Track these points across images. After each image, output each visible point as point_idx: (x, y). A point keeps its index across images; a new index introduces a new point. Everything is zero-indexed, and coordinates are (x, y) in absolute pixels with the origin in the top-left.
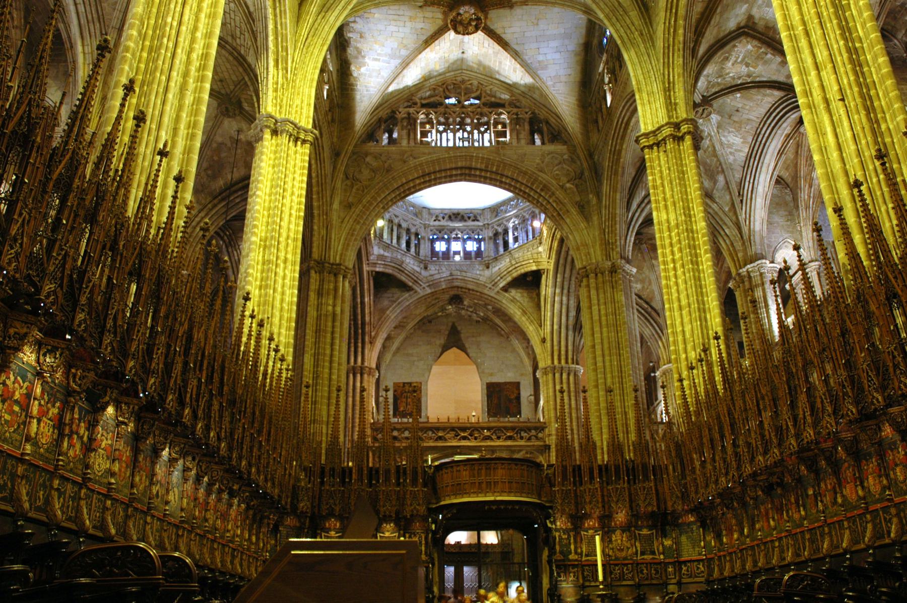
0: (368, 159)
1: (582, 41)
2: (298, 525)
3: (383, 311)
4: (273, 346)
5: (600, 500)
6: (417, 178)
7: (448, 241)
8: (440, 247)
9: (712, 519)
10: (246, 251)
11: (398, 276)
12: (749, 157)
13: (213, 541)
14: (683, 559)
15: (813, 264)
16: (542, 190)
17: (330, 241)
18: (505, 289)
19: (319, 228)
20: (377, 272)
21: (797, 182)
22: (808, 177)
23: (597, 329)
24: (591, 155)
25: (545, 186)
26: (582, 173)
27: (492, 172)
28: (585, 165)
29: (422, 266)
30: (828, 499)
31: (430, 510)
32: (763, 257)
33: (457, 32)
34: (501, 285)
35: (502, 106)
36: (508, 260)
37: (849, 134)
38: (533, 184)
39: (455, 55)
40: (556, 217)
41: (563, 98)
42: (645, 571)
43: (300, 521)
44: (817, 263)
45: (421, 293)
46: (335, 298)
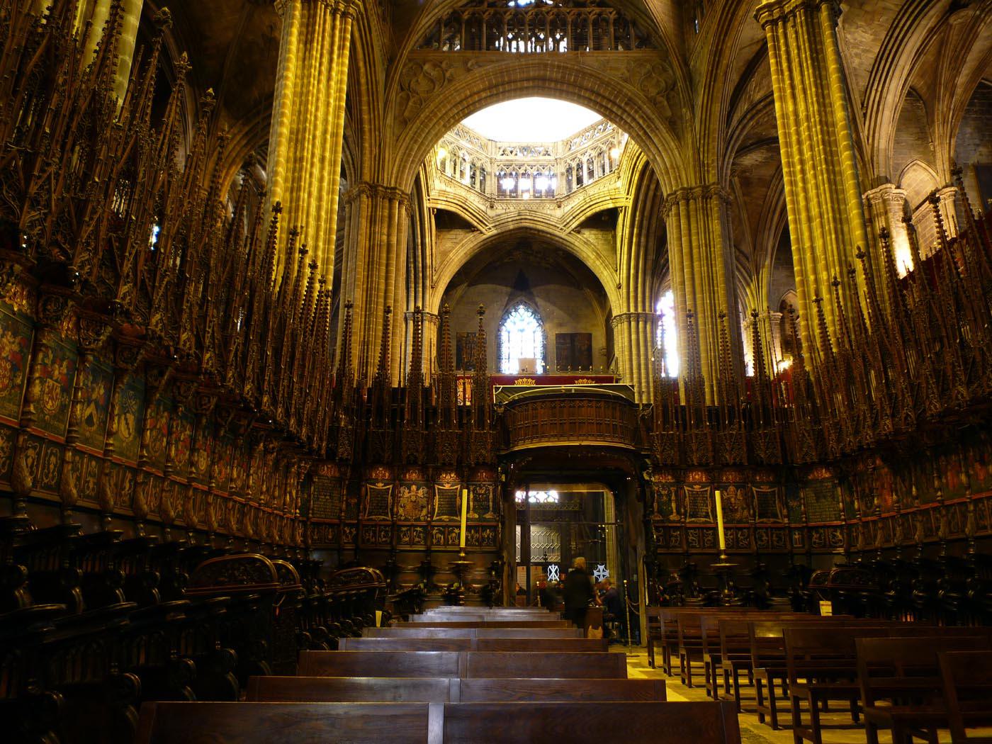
0: (426, 67)
2: (337, 475)
4: (308, 261)
5: (711, 449)
6: (484, 90)
8: (508, 184)
9: (855, 475)
10: (274, 145)
12: (879, 59)
13: (208, 493)
14: (812, 524)
15: (949, 189)
16: (626, 104)
17: (384, 161)
19: (371, 147)
20: (438, 210)
21: (934, 91)
22: (950, 85)
25: (630, 99)
26: (675, 84)
27: (569, 84)
28: (679, 73)
29: (488, 204)
32: (888, 181)
34: (573, 226)
36: (582, 198)
38: (616, 97)
40: (642, 137)
42: (765, 538)
43: (339, 471)
44: (953, 189)
46: (390, 226)
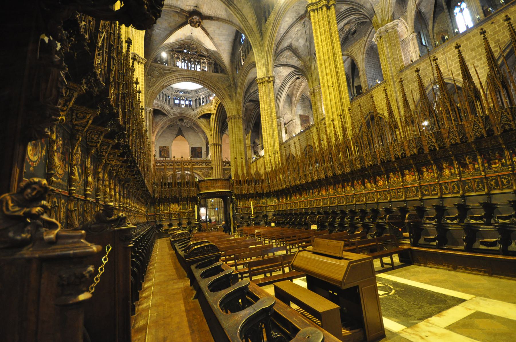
1: (233, 38)
3: (157, 123)
7: (180, 100)
8: (177, 102)
11: (162, 111)
12: (281, 87)
18: (199, 118)
23: (234, 136)
24: (234, 80)
26: (230, 85)
28: (232, 82)
30: (316, 193)
31: (197, 194)
33: (191, 26)
35: (205, 57)
37: (333, 97)
39: (189, 34)
41: (226, 58)
45: (171, 117)
